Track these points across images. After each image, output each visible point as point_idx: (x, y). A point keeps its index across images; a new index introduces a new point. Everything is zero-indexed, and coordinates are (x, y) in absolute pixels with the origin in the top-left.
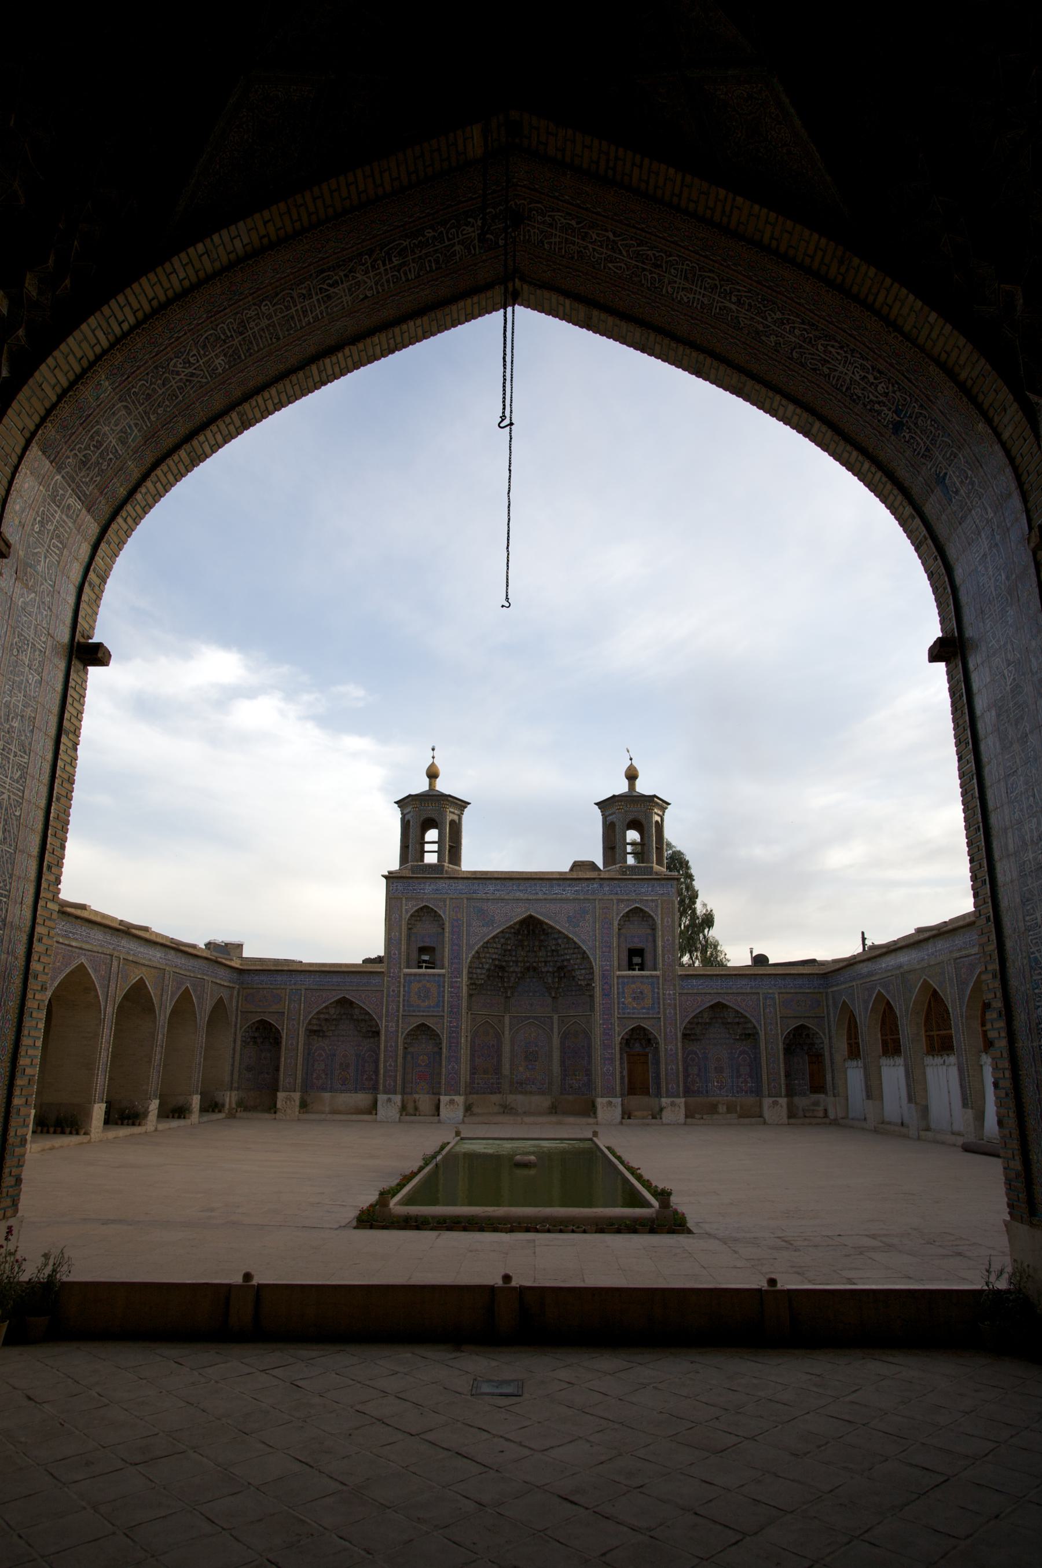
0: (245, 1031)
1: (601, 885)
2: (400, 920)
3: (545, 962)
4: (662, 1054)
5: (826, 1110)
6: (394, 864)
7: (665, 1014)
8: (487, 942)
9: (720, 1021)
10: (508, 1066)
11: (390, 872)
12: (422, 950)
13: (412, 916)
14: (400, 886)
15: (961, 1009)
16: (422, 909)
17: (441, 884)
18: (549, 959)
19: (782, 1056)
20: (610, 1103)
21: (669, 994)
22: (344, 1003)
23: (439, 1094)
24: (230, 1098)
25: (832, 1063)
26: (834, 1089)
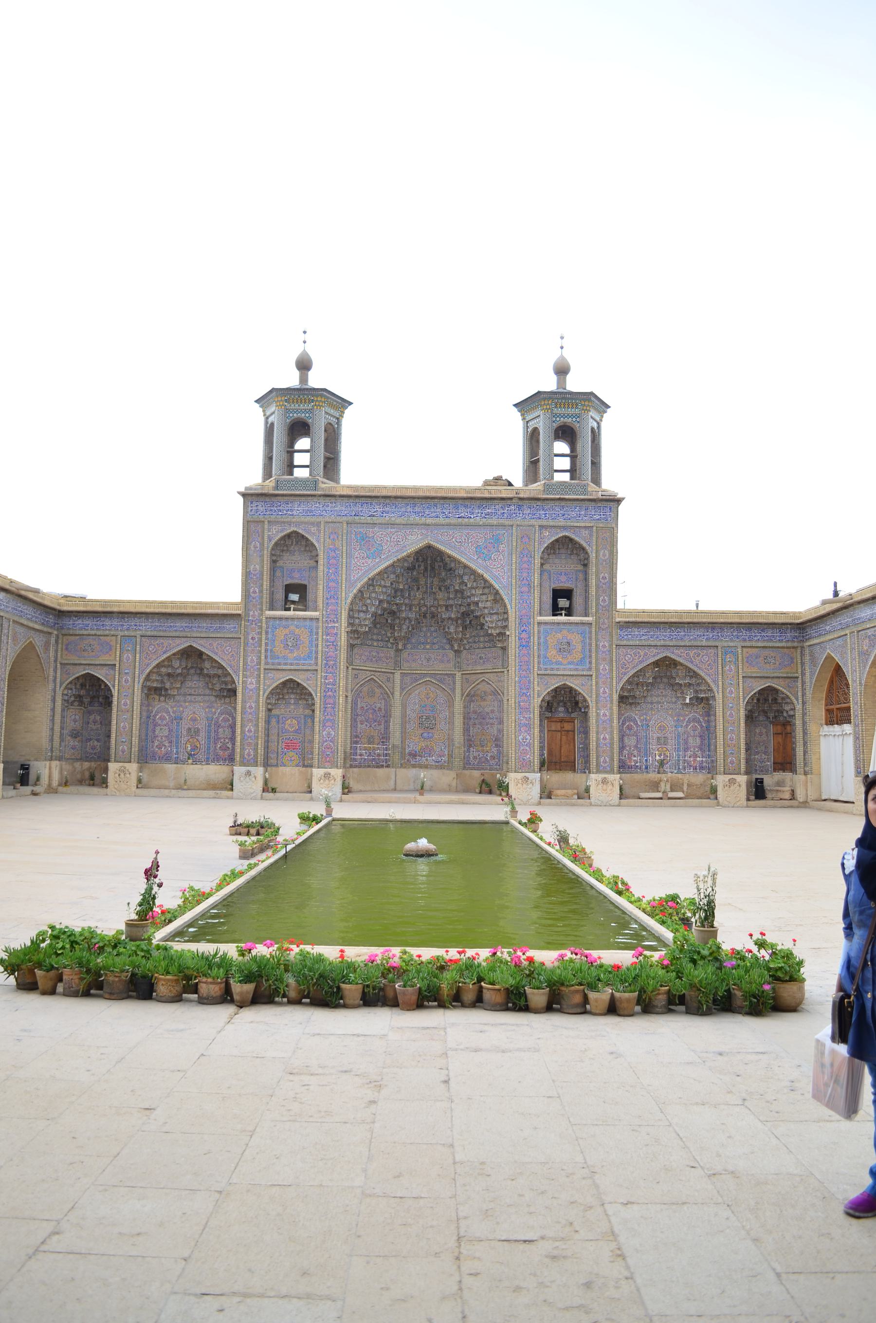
0: (66, 688)
1: (520, 507)
2: (262, 550)
3: (447, 607)
4: (593, 721)
5: (793, 792)
6: (253, 475)
7: (597, 670)
8: (372, 579)
10: (398, 734)
11: (246, 488)
12: (290, 588)
13: (276, 544)
16: (289, 536)
17: (315, 506)
18: (451, 602)
19: (743, 724)
21: (604, 646)
22: (192, 655)
23: (312, 766)
24: (47, 770)
25: (805, 733)
26: (805, 764)
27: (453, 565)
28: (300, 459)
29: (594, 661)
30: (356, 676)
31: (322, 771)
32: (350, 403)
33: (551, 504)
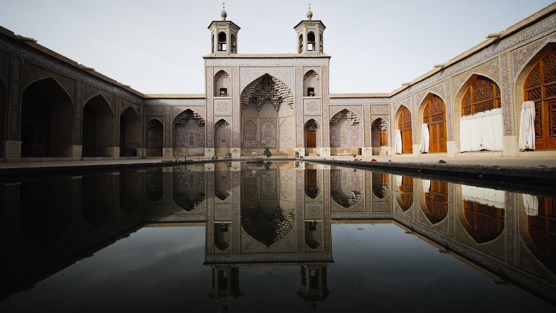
10: (259, 138)
12: (222, 89)
13: (216, 75)
14: (210, 62)
15: (512, 77)
28: (224, 47)
30: (244, 119)
31: (234, 149)
32: (240, 28)
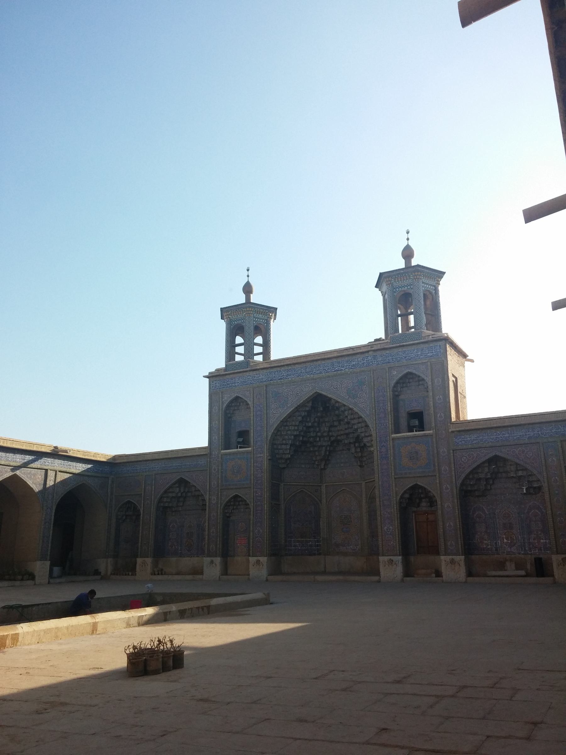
1: (375, 357)
3: (347, 434)
9: (504, 475)
11: (210, 373)
18: (347, 431)
20: (391, 562)
27: (337, 405)
29: (436, 464)
33: (396, 351)
